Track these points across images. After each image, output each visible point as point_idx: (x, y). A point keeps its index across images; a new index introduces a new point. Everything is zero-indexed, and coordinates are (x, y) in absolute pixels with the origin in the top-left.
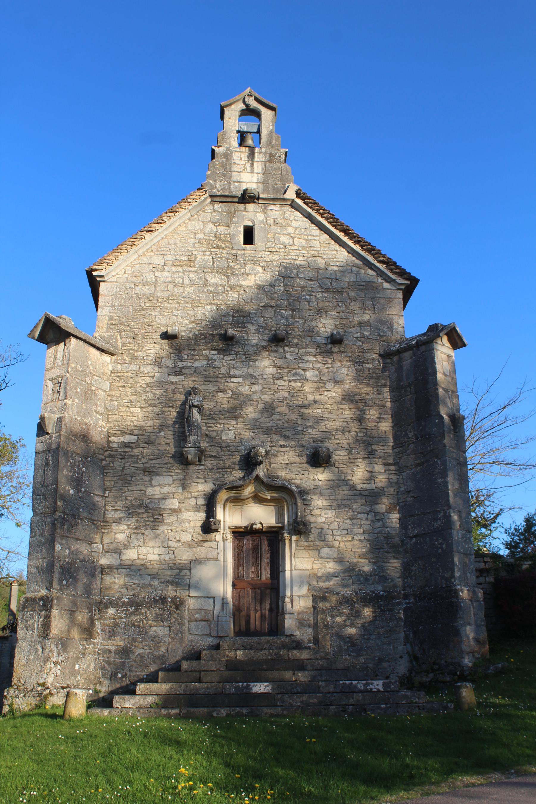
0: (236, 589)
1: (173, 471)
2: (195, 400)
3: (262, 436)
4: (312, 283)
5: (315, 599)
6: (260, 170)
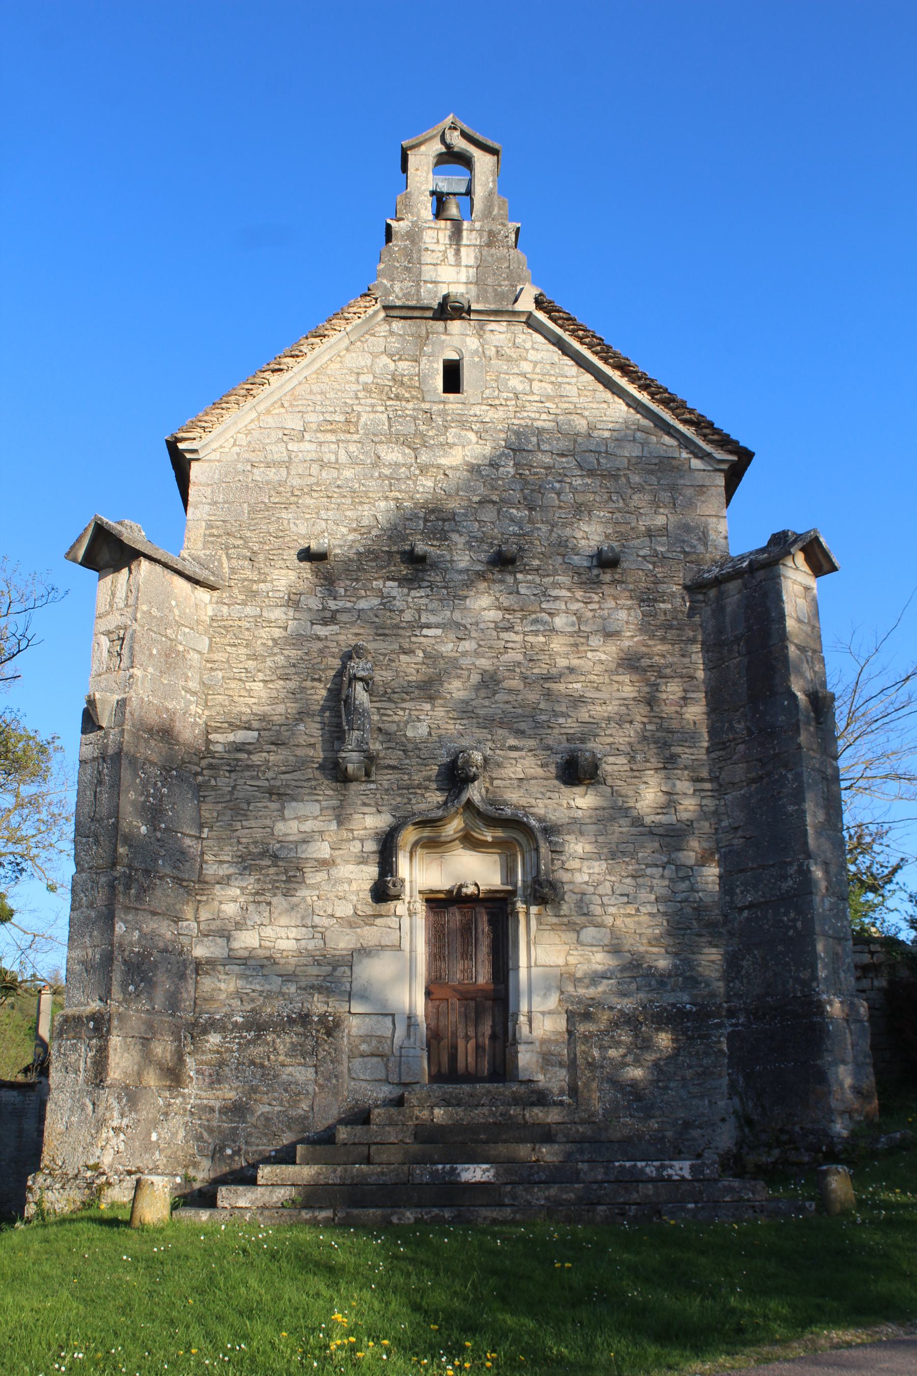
0: (432, 1000)
1: (321, 792)
2: (358, 667)
3: (477, 731)
4: (564, 460)
5: (571, 1016)
6: (472, 262)
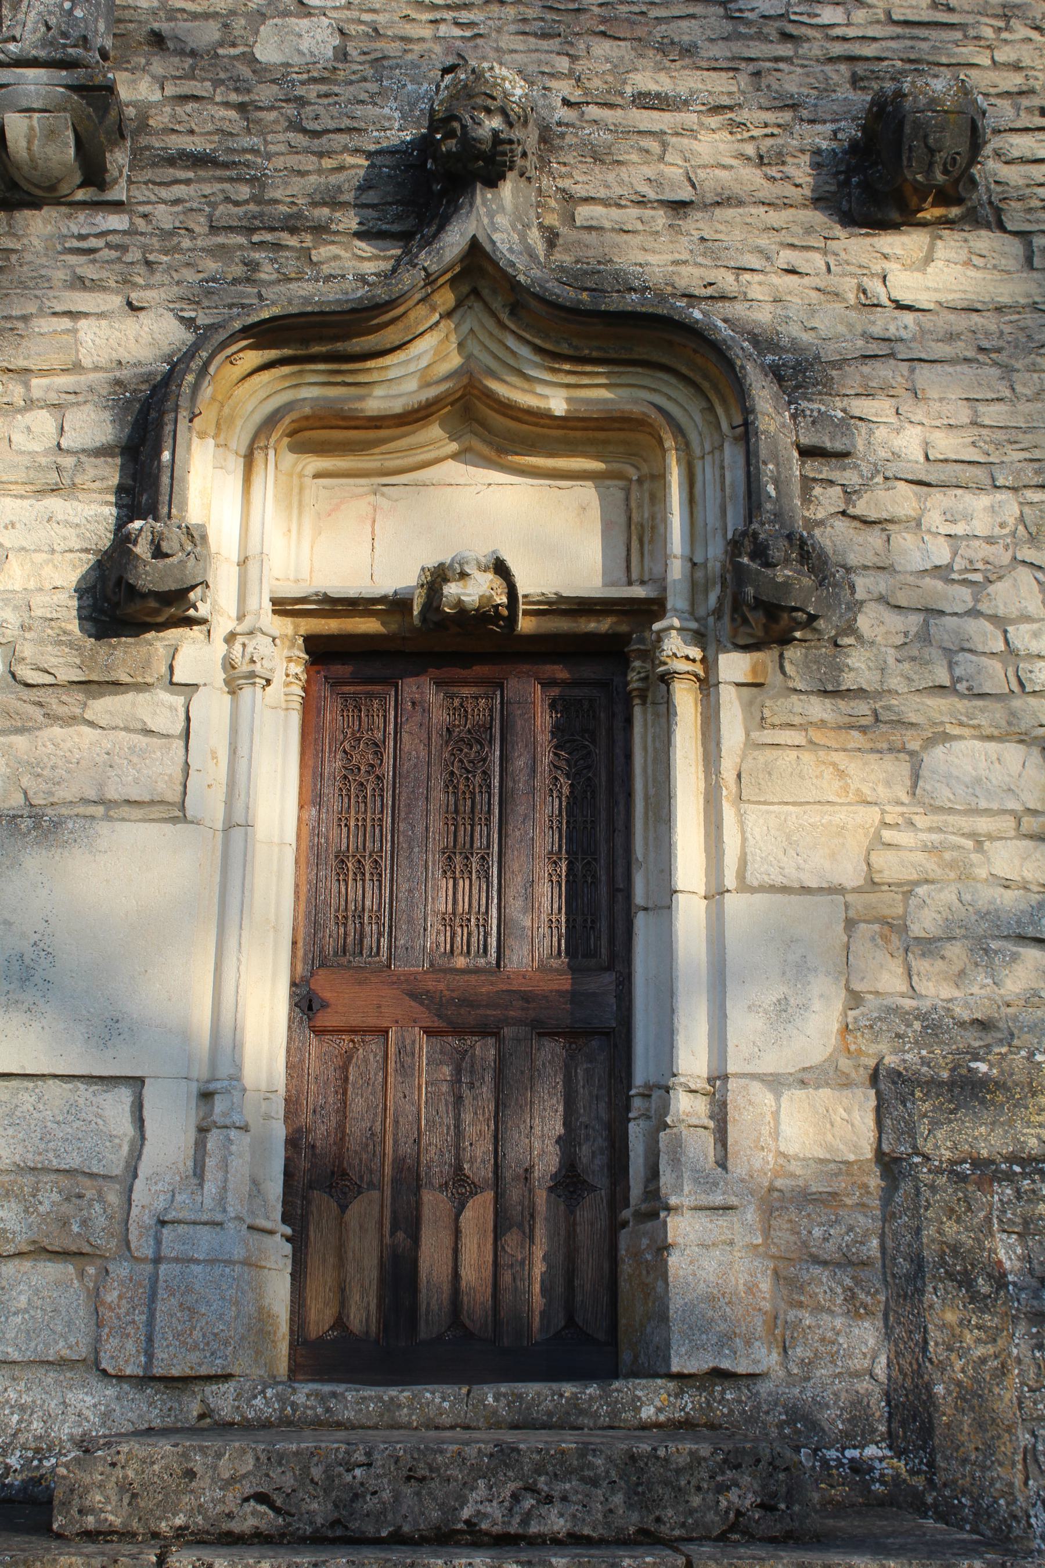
3: (518, 43)
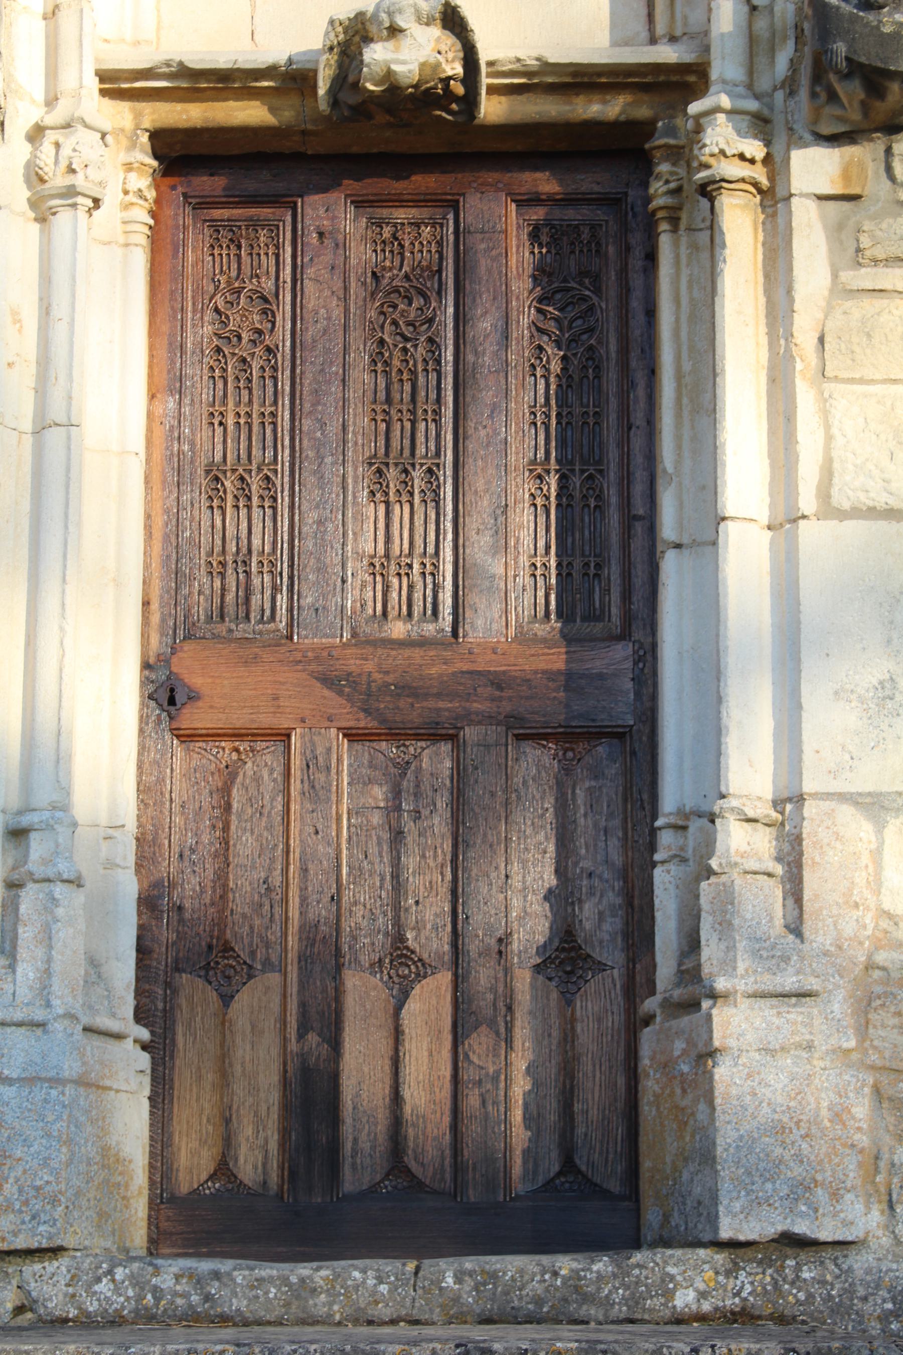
0: (186, 737)
